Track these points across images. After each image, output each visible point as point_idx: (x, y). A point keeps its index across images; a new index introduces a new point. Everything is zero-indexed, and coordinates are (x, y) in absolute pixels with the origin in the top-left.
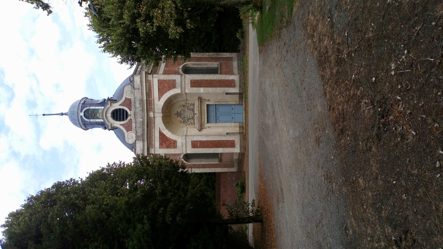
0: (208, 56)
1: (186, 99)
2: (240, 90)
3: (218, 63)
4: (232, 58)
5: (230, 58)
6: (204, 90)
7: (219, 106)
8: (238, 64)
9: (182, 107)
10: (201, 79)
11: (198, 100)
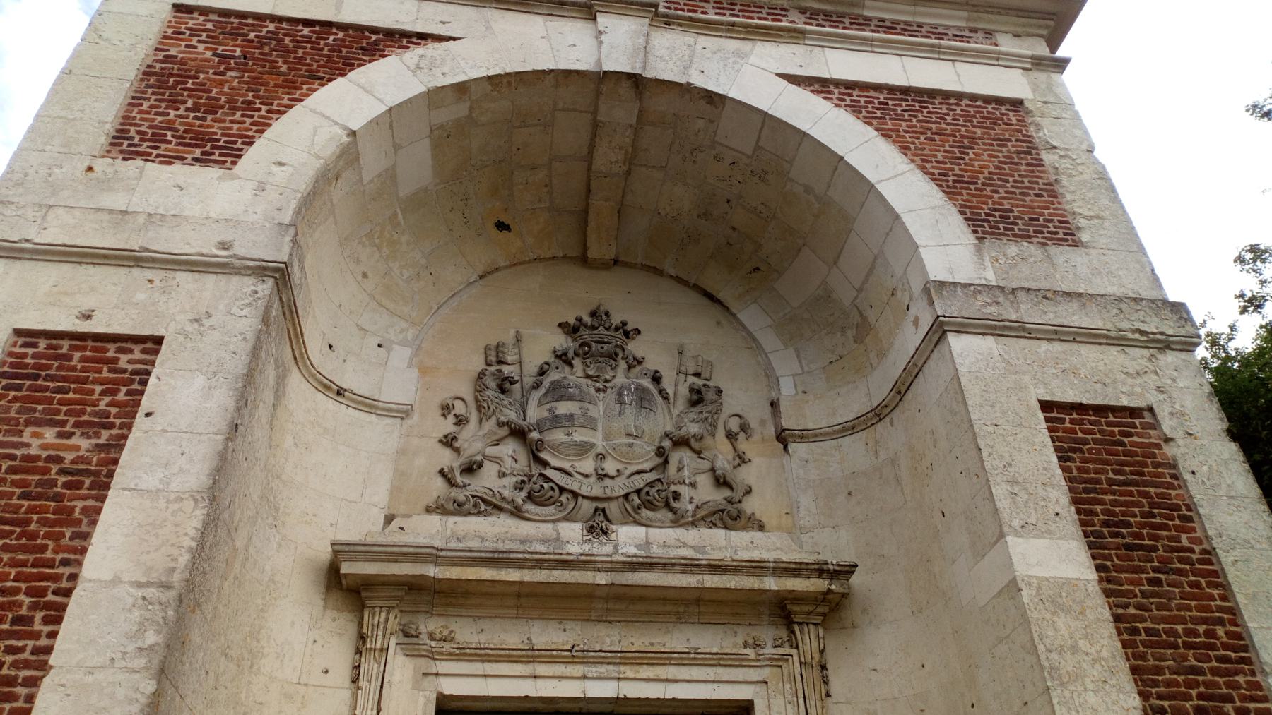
1: (804, 435)
11: (820, 570)
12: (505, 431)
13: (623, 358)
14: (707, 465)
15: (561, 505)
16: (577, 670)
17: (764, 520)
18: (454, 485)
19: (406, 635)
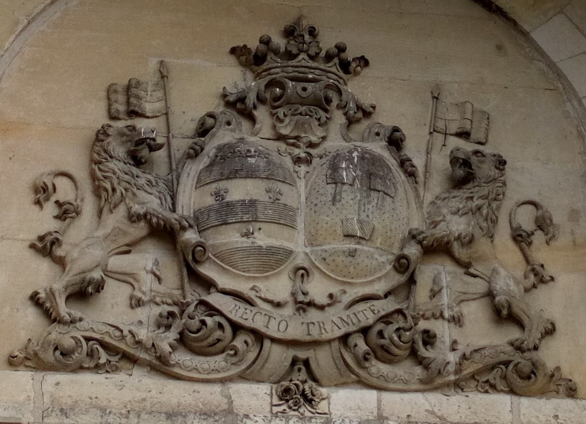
12: (140, 229)
13: (339, 107)
14: (479, 286)
15: (236, 354)
17: (577, 379)
18: (55, 321)
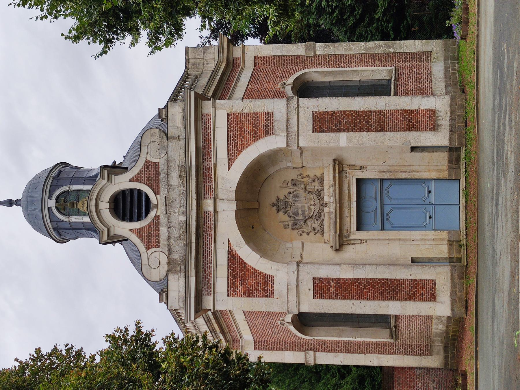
0: (364, 52)
1: (302, 163)
2: (451, 139)
3: (391, 68)
4: (428, 55)
5: (424, 53)
6: (350, 140)
7: (391, 185)
8: (446, 69)
9: (290, 184)
10: (342, 109)
11: (334, 166)
14: (310, 183)
16: (352, 208)
19: (347, 237)
